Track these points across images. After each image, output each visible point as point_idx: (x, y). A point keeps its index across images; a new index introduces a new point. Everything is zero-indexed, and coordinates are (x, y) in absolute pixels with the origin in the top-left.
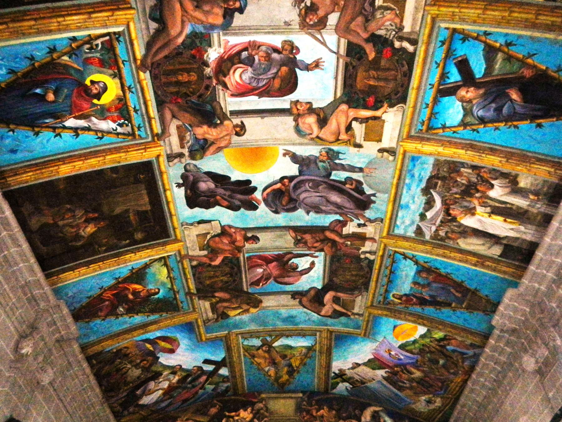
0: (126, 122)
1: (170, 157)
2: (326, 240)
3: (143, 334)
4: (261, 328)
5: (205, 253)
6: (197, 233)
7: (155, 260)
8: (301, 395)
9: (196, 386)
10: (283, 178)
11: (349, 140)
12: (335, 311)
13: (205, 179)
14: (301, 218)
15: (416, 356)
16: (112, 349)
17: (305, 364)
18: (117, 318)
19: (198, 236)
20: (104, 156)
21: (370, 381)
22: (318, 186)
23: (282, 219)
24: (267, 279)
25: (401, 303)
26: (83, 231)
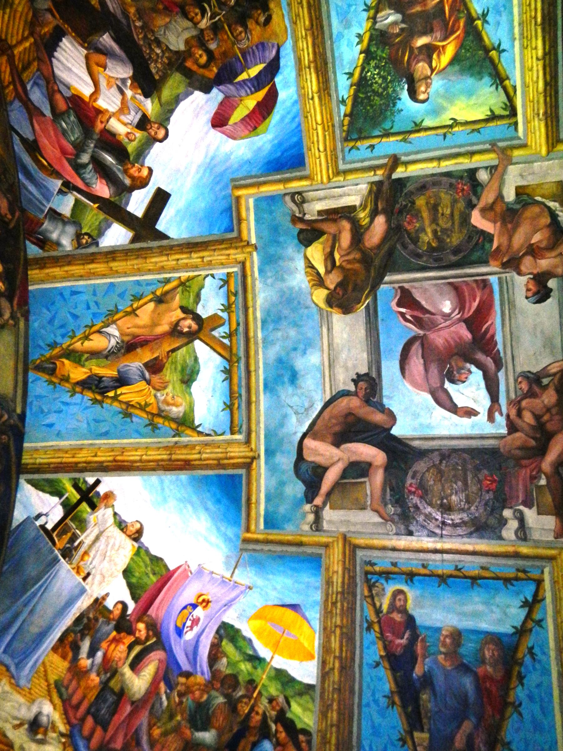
3: (299, 60)
4: (258, 314)
5: (510, 195)
7: (510, 99)
8: (19, 411)
9: (79, 175)
12: (319, 471)
15: (206, 668)
17: (127, 415)
18: (368, 9)
21: (78, 570)
24: (418, 322)
25: (378, 611)
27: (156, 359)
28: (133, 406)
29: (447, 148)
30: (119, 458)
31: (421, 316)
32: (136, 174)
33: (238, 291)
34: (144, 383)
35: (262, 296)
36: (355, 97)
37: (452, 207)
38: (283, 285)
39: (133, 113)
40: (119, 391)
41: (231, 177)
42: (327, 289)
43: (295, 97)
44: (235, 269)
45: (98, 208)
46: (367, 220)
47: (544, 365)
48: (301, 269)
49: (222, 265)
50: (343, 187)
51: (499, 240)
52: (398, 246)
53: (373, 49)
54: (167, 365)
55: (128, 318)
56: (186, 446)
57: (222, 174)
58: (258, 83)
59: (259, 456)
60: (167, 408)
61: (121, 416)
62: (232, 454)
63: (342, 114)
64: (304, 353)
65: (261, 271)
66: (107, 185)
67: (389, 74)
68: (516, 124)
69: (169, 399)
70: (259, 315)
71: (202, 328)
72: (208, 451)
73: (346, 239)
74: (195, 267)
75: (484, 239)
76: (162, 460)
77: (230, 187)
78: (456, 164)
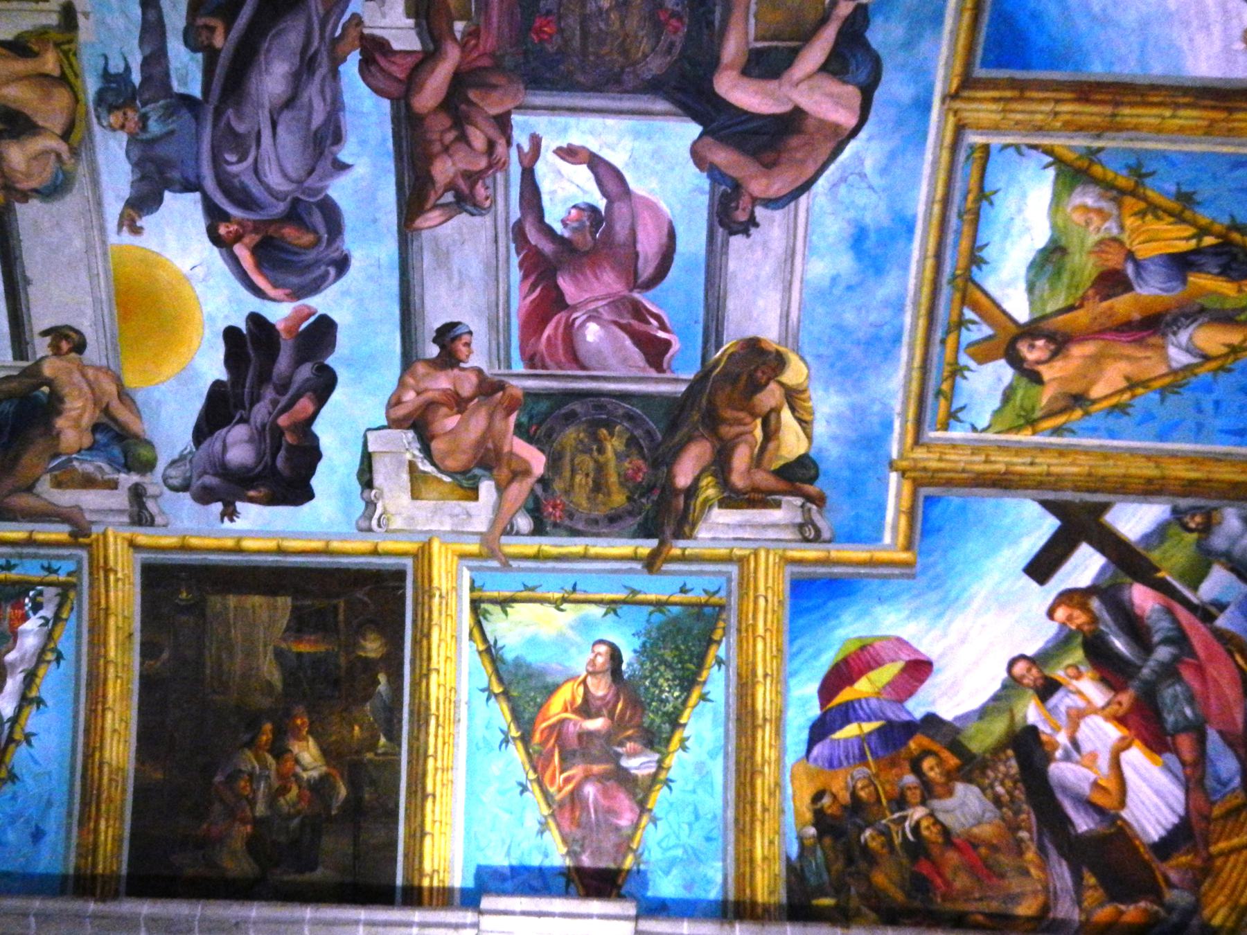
0: (31, 593)
1: (140, 516)
2: (455, 104)
3: (779, 732)
5: (487, 489)
6: (405, 498)
10: (216, 239)
11: (57, 45)
12: (835, 66)
13: (218, 446)
14: (364, 183)
16: (801, 839)
17: (1187, 198)
19: (415, 496)
20: (107, 663)
22: (237, 135)
23: (371, 248)
24: (639, 312)
26: (305, 770)
27: (1105, 298)
28: (1171, 214)
29: (572, 571)
30: (1222, 115)
31: (633, 322)
32: (1077, 613)
33: (934, 397)
34: (1140, 255)
35: (893, 385)
36: (700, 666)
37: (572, 486)
38: (857, 398)
39: (1063, 709)
40: (1193, 244)
41: (911, 582)
42: (782, 384)
43: (792, 682)
44: (933, 434)
45: (1158, 570)
46: (704, 483)
47: (450, 222)
48: (819, 422)
49: (954, 445)
50: (736, 539)
51: (507, 425)
52: (659, 436)
53: (667, 727)
54: (1089, 284)
55: (1147, 376)
56: (1081, 129)
57: (930, 588)
58: (847, 714)
59: (943, 101)
60: (1104, 204)
61: (1198, 198)
62: (994, 107)
63: (723, 645)
64: (834, 280)
65: (888, 426)
66: (1132, 604)
67: (647, 689)
68: (472, 589)
69: (1096, 220)
70: (904, 354)
71: (1009, 343)
72: (1039, 117)
73: (741, 459)
74: (1003, 447)
75: (528, 432)
76: (1132, 105)
77: (918, 566)
78: (561, 546)
